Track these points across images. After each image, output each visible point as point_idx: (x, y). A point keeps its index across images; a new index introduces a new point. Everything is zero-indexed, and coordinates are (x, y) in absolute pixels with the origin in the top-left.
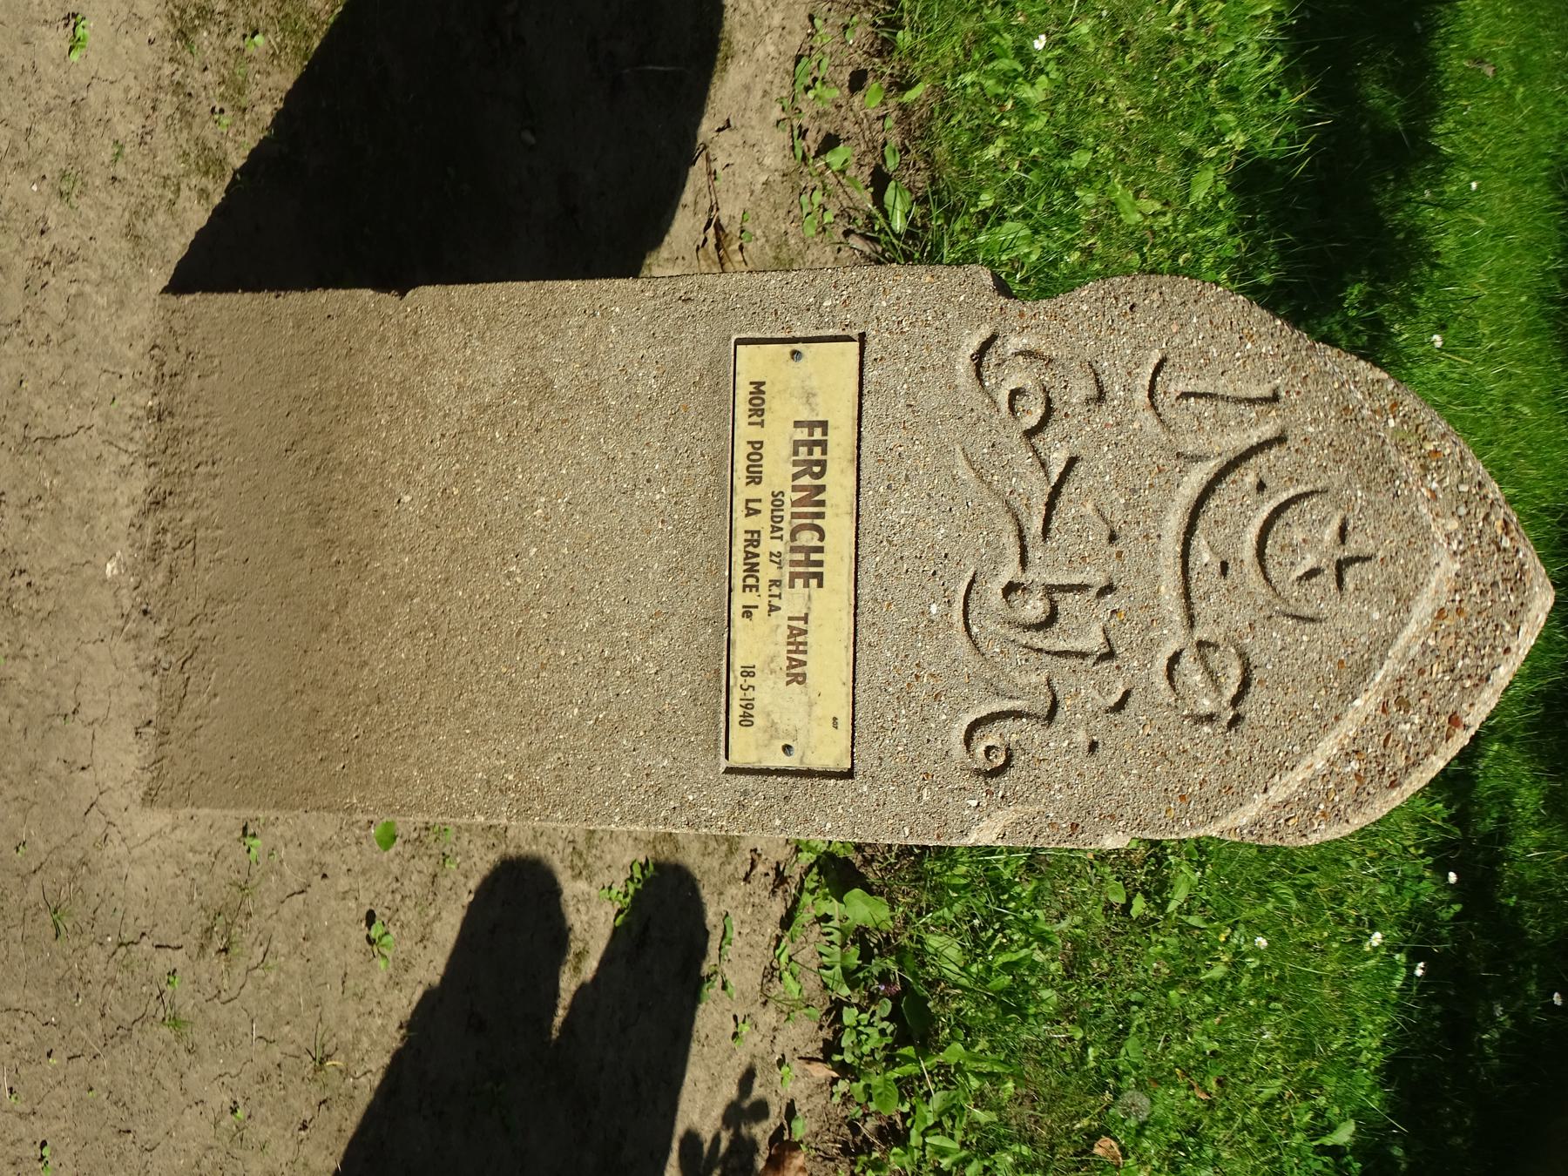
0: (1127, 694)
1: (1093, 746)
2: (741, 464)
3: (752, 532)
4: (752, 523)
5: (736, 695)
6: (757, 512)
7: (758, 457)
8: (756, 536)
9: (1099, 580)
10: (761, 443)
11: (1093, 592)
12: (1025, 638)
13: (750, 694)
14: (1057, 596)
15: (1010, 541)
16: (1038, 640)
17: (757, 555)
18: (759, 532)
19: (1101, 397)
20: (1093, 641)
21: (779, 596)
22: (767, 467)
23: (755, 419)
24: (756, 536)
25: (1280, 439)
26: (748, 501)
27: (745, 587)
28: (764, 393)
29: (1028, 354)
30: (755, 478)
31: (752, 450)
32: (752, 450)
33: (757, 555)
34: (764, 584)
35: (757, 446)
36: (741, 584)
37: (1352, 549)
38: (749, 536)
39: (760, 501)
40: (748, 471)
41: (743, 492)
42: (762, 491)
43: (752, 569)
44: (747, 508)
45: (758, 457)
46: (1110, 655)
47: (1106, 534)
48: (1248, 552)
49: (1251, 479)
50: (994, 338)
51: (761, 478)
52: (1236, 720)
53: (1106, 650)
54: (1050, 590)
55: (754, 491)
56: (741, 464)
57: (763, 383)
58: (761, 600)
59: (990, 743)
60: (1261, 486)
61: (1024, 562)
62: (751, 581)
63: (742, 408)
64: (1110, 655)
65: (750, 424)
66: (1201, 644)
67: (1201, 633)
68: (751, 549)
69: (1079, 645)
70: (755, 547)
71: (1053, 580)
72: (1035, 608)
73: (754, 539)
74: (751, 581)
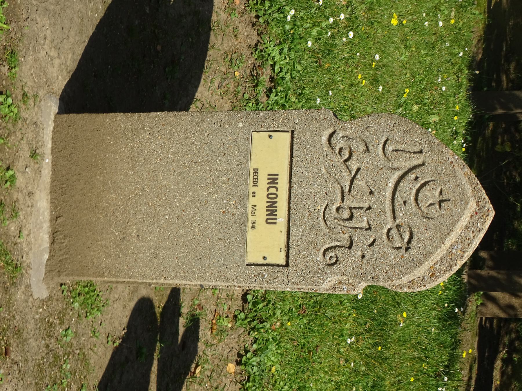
1: (363, 256)
9: (366, 205)
16: (346, 224)
19: (368, 150)
46: (370, 228)
50: (334, 132)
52: (407, 249)
53: (368, 227)
54: (350, 208)
59: (330, 255)
61: (343, 199)
64: (370, 228)
66: (398, 226)
67: (398, 222)
71: (352, 206)
72: (346, 215)
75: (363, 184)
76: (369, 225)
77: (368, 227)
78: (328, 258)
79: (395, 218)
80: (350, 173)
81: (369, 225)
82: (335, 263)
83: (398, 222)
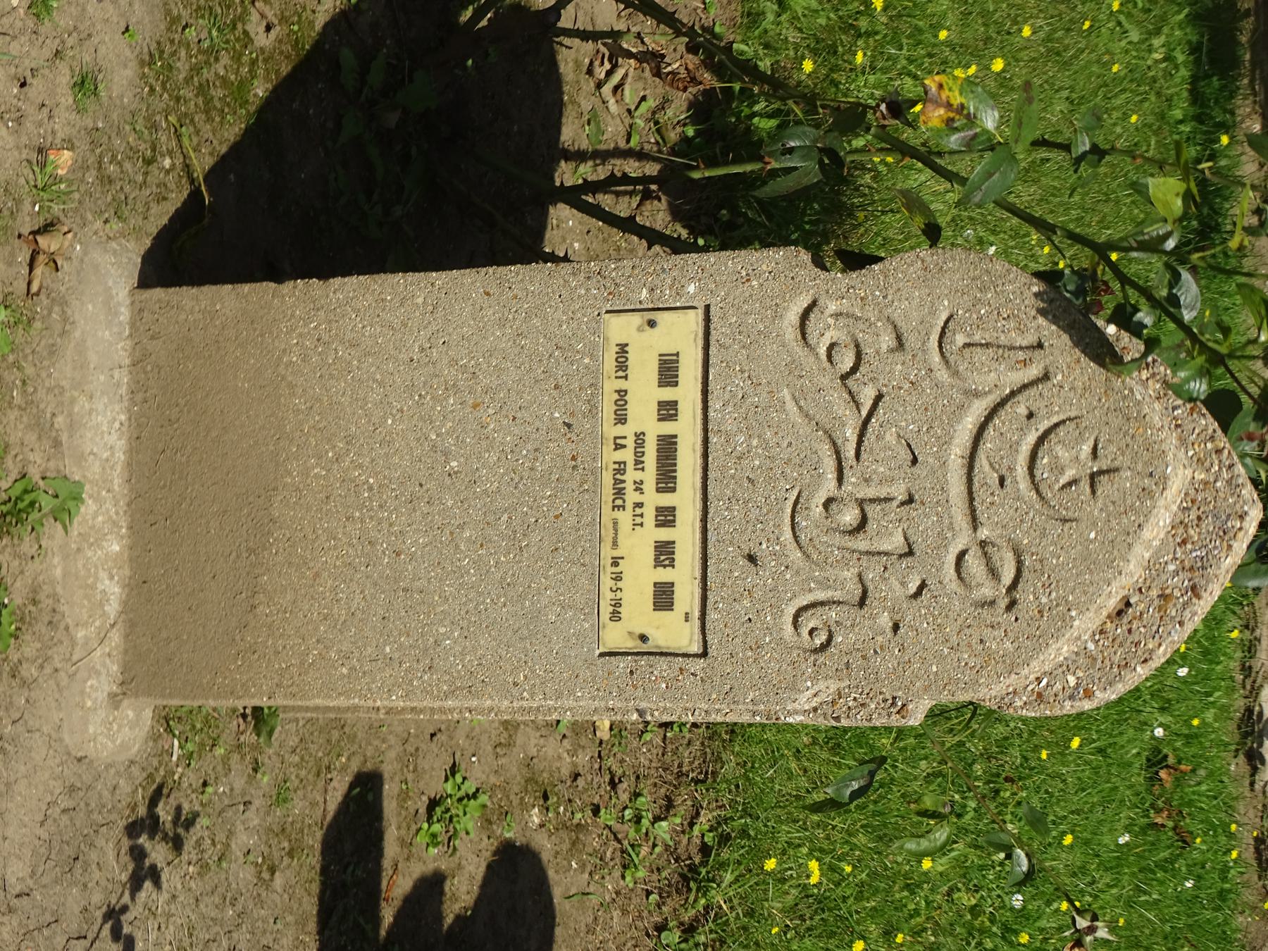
0: (923, 585)
3: (619, 463)
4: (619, 455)
5: (607, 596)
6: (624, 446)
7: (623, 403)
8: (622, 466)
10: (626, 391)
11: (895, 503)
12: (838, 539)
13: (619, 595)
14: (868, 508)
15: (829, 464)
17: (624, 481)
18: (625, 463)
20: (896, 542)
21: (642, 515)
22: (632, 410)
23: (621, 374)
24: (622, 466)
25: (1046, 377)
26: (616, 438)
27: (614, 507)
28: (627, 352)
29: (837, 315)
30: (621, 419)
31: (616, 396)
32: (616, 396)
33: (624, 481)
34: (629, 505)
35: (622, 394)
36: (611, 504)
37: (1104, 464)
38: (617, 466)
39: (625, 437)
40: (616, 414)
42: (628, 430)
43: (619, 493)
44: (616, 444)
45: (623, 403)
47: (905, 455)
48: (1021, 470)
49: (1022, 410)
50: (814, 303)
51: (626, 419)
53: (907, 550)
54: (861, 503)
55: (620, 430)
57: (627, 345)
58: (625, 518)
59: (811, 625)
60: (1030, 416)
61: (840, 479)
62: (619, 502)
64: (910, 553)
65: (616, 377)
66: (983, 544)
67: (984, 533)
68: (618, 476)
69: (886, 547)
70: (622, 474)
72: (849, 517)
73: (620, 468)
74: (619, 502)
75: (890, 437)
76: (909, 546)
77: (907, 550)
78: (805, 632)
79: (975, 523)
80: (858, 406)
81: (909, 546)
82: (824, 647)
83: (984, 533)
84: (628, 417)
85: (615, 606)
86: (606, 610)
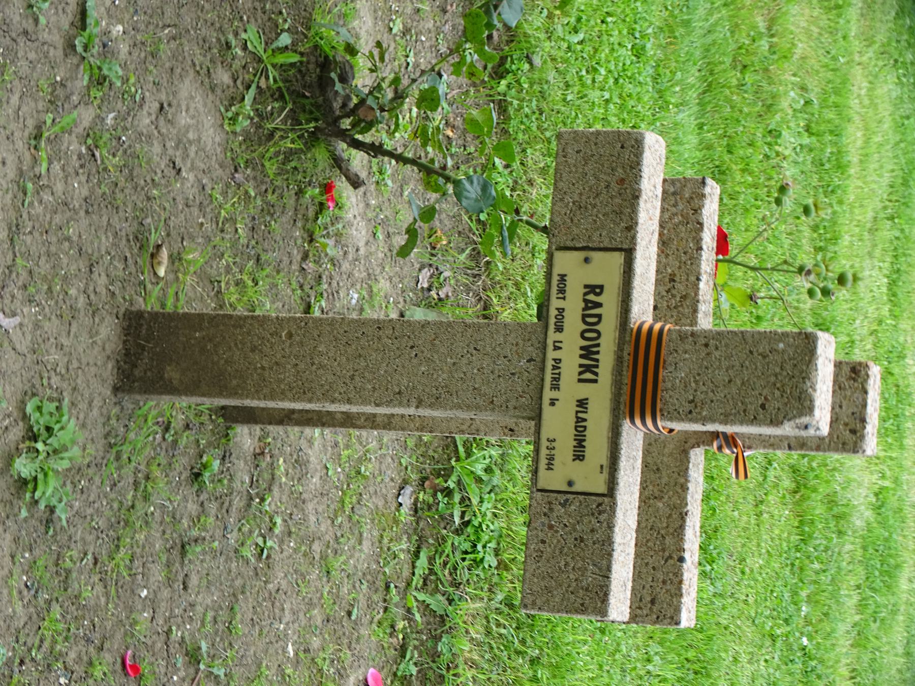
2: (552, 321)
4: (557, 354)
5: (544, 452)
6: (560, 348)
13: (553, 452)
23: (561, 295)
26: (555, 342)
30: (559, 329)
31: (556, 312)
32: (556, 312)
41: (552, 336)
43: (556, 379)
44: (554, 346)
55: (558, 336)
56: (552, 321)
57: (565, 275)
63: (554, 289)
84: (565, 328)
85: (549, 459)
86: (543, 462)
